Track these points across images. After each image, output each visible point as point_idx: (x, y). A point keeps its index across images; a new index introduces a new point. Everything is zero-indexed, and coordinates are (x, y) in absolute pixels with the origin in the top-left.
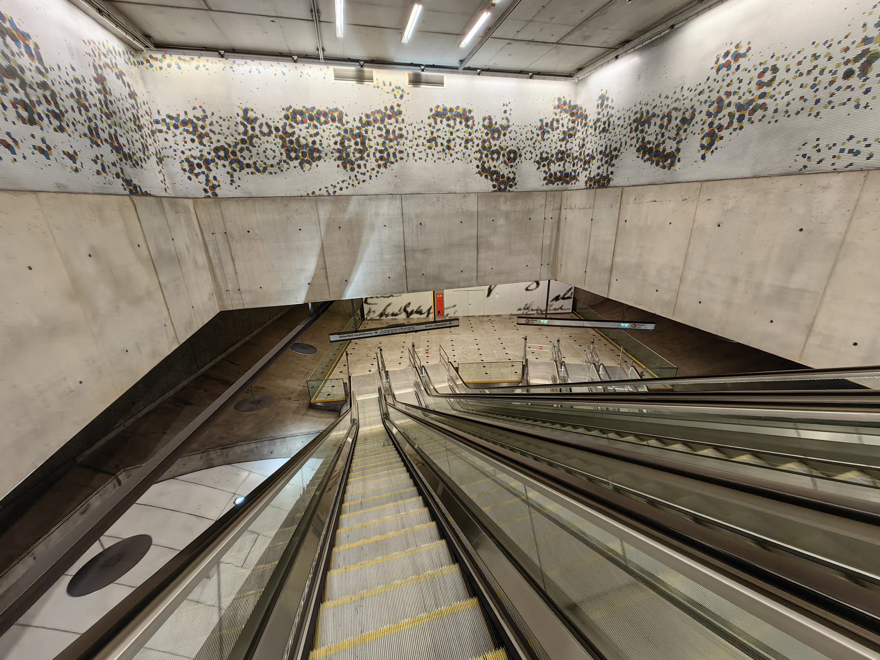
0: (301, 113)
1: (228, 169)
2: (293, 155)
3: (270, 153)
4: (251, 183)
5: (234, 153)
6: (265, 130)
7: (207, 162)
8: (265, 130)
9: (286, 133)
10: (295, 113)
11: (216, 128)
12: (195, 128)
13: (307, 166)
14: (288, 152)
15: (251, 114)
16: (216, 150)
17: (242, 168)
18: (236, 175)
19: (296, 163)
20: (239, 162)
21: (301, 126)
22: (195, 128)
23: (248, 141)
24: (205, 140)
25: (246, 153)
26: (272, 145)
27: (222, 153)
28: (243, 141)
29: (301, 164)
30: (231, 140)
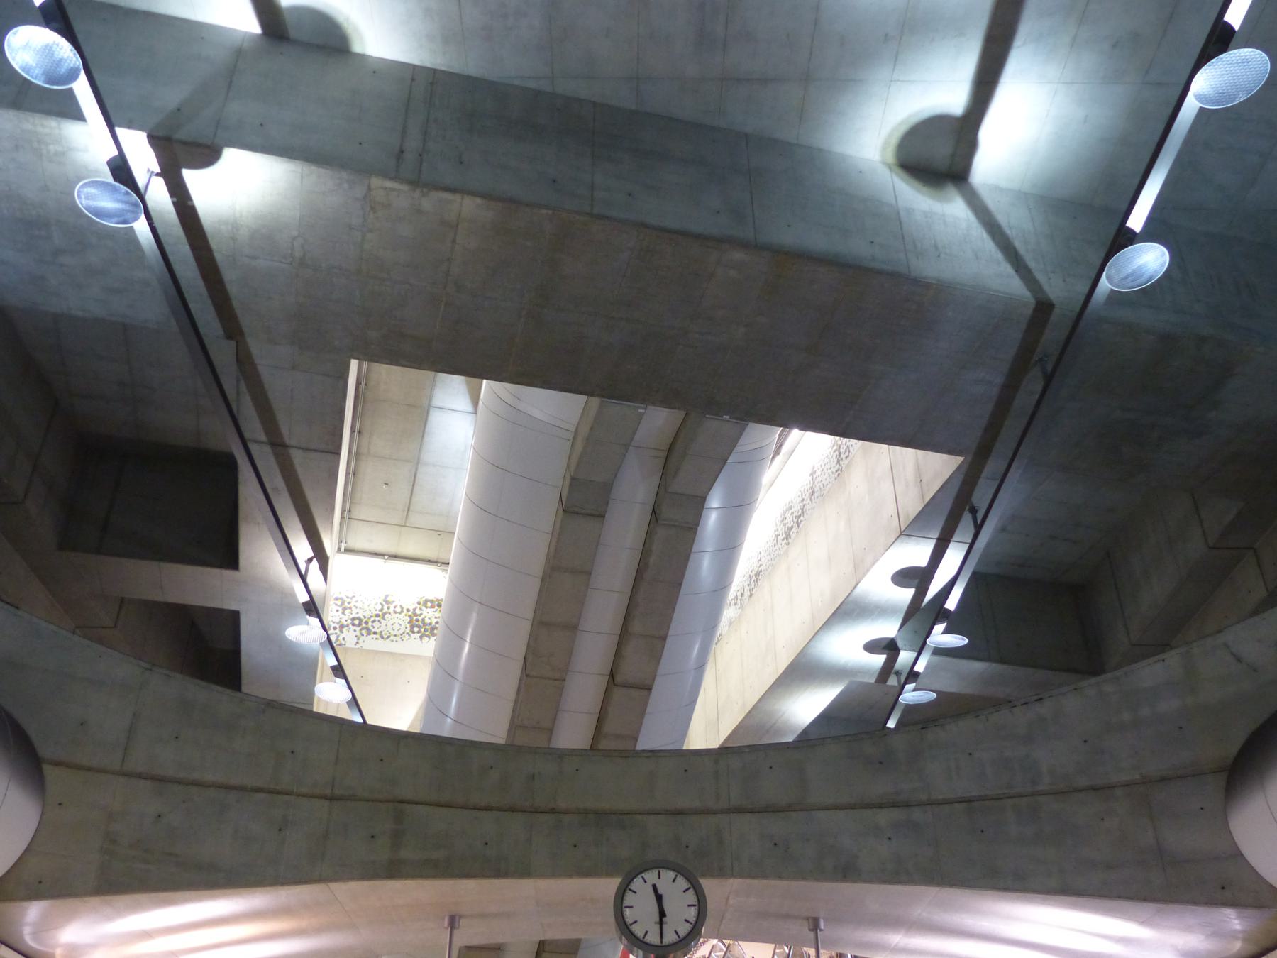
0: (432, 602)
1: (358, 633)
2: (416, 629)
3: (396, 627)
4: (369, 643)
5: (366, 623)
6: (398, 609)
7: (342, 627)
8: (398, 609)
9: (415, 614)
10: (426, 601)
11: (359, 605)
12: (343, 603)
13: (426, 639)
14: (412, 627)
15: (389, 599)
16: (353, 619)
17: (369, 634)
18: (362, 638)
19: (417, 636)
20: (368, 629)
21: (430, 610)
22: (343, 603)
23: (381, 616)
24: (347, 612)
25: (376, 624)
26: (402, 621)
27: (357, 622)
28: (377, 615)
29: (421, 637)
30: (367, 614)
